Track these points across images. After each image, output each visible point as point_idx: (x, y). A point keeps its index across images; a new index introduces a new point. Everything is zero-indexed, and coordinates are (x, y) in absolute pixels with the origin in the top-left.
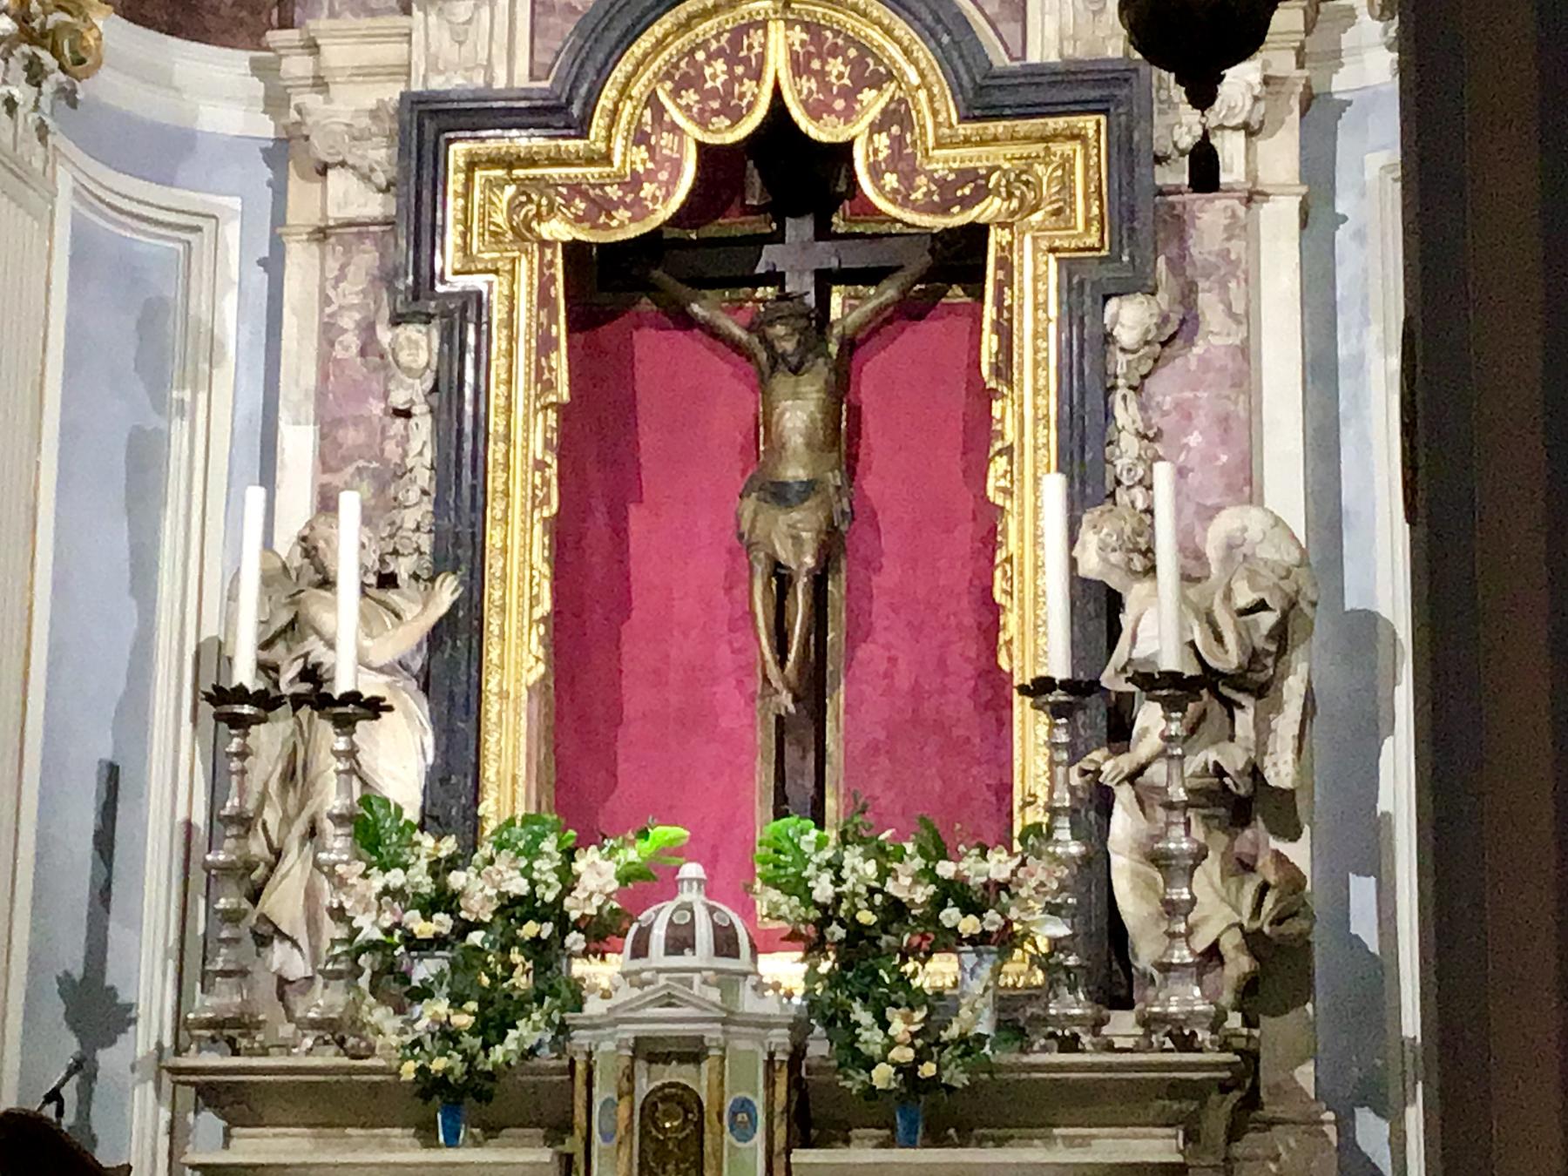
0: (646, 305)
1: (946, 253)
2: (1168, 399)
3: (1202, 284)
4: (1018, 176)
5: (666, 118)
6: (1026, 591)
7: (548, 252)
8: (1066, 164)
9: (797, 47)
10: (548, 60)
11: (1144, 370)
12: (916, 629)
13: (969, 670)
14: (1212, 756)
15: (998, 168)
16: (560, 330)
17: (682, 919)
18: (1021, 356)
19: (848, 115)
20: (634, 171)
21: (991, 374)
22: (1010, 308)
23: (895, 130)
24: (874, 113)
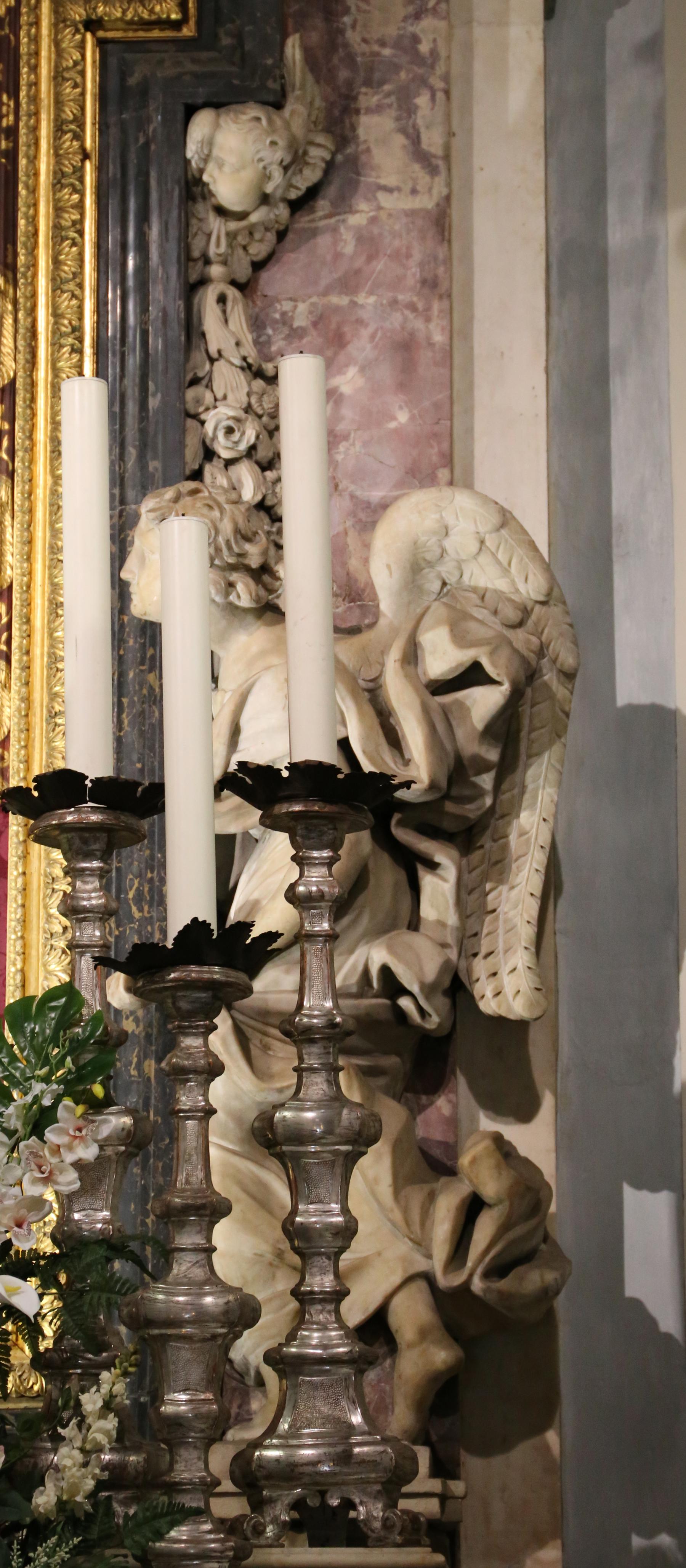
2: (302, 307)
3: (368, 99)
11: (259, 250)
14: (377, 955)
18: (33, 221)
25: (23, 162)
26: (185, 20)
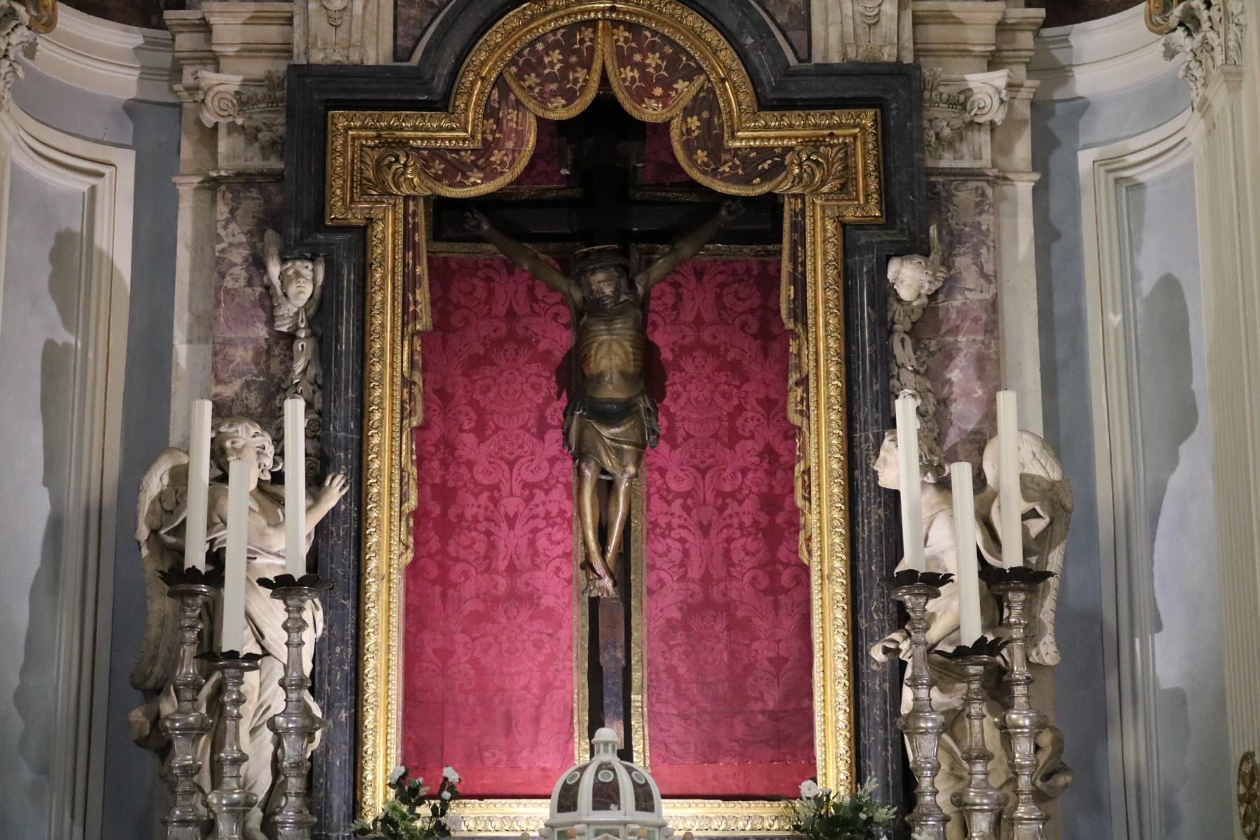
1: (730, 219)
2: (933, 342)
5: (512, 97)
10: (410, 44)
12: (705, 529)
13: (749, 562)
16: (422, 270)
17: (606, 777)
22: (804, 264)
24: (686, 100)
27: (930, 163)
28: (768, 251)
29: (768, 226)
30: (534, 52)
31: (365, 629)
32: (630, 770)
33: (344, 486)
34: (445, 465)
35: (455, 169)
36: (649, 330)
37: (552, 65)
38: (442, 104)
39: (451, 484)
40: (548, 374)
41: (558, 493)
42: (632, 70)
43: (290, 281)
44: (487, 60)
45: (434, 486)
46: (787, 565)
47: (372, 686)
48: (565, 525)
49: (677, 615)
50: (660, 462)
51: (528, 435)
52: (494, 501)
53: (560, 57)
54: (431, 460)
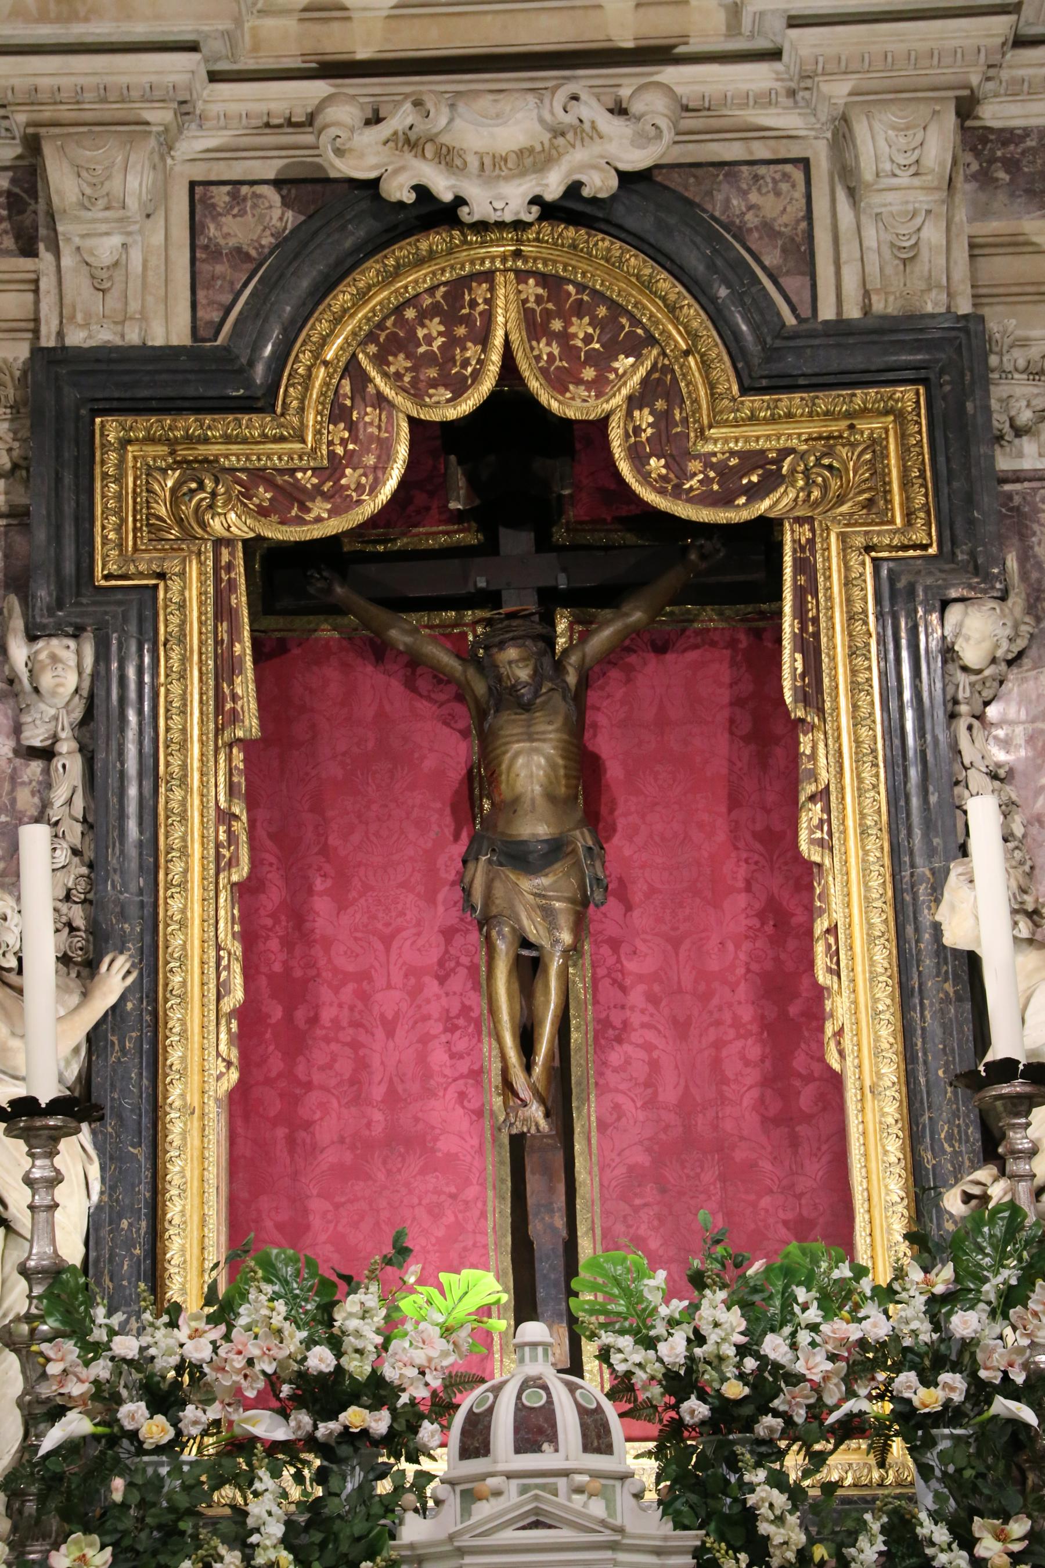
0: (327, 632)
1: (704, 565)
4: (818, 459)
5: (371, 389)
6: (859, 969)
7: (225, 553)
8: (876, 446)
9: (531, 305)
11: (987, 694)
12: (681, 1028)
13: (752, 1076)
15: (792, 451)
16: (244, 648)
17: (535, 1400)
18: (834, 678)
19: (600, 386)
20: (332, 455)
21: (796, 701)
22: (816, 621)
23: (660, 405)
25: (824, 640)
26: (930, 545)
27: (1004, 463)
28: (762, 613)
29: (759, 576)
30: (401, 321)
31: (165, 1191)
32: (572, 1388)
33: (129, 972)
34: (288, 944)
35: (290, 498)
36: (587, 735)
37: (429, 339)
38: (262, 401)
39: (298, 973)
40: (438, 805)
41: (458, 982)
42: (549, 344)
43: (43, 668)
44: (336, 337)
45: (271, 976)
46: (809, 1079)
47: (177, 1279)
48: (471, 1029)
49: (640, 1157)
50: (612, 929)
51: (411, 896)
52: (364, 997)
53: (442, 328)
54: (267, 938)
